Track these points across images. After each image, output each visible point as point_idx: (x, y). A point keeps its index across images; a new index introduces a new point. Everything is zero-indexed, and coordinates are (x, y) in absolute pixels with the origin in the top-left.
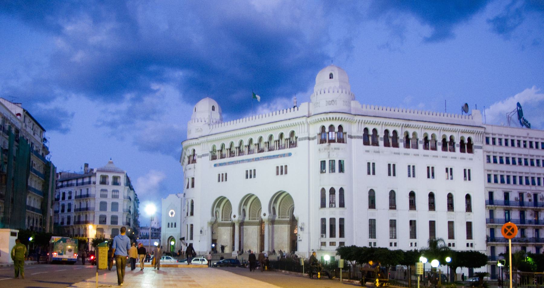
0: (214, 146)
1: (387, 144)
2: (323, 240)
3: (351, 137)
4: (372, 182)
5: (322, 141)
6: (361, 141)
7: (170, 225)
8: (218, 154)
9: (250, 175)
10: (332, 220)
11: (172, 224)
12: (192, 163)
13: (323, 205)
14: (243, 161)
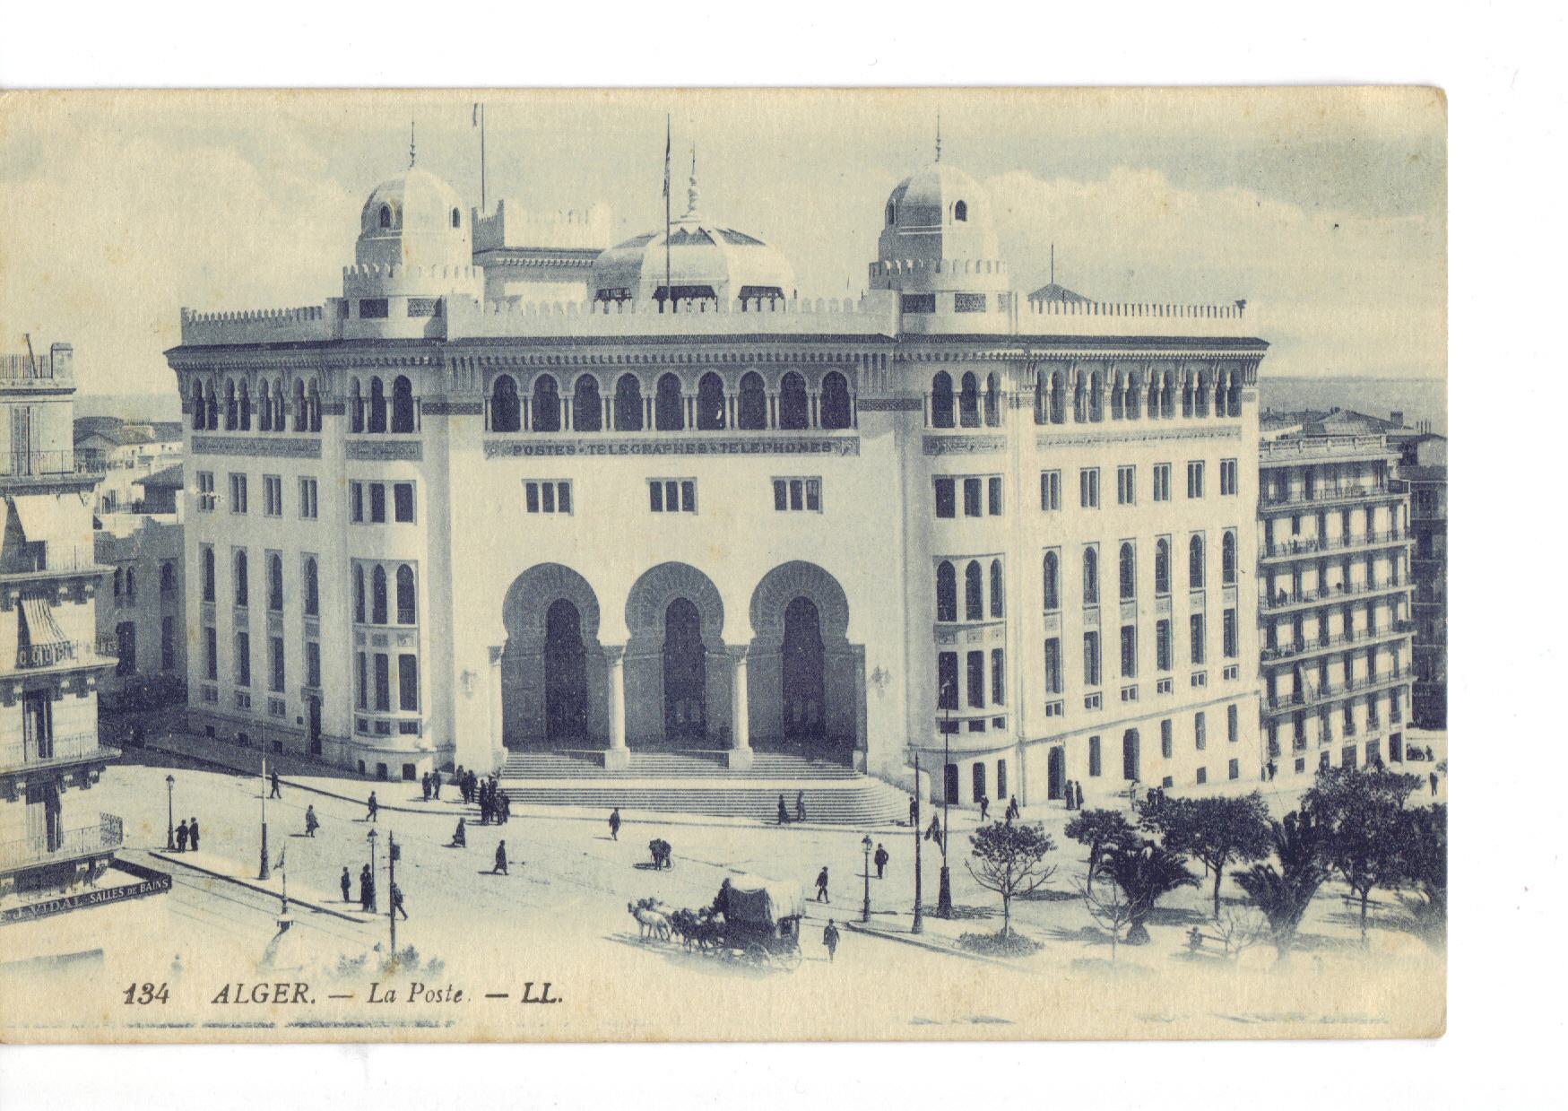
0: (504, 384)
9: (672, 497)
10: (975, 658)
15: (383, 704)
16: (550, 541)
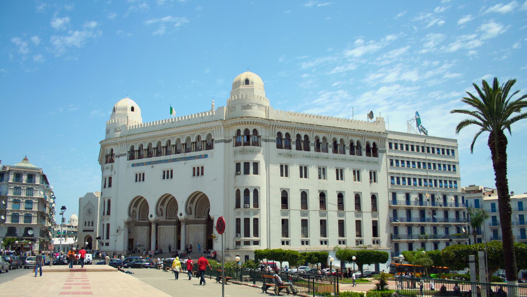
1: (299, 148)
3: (266, 141)
4: (284, 183)
5: (238, 144)
6: (275, 144)
7: (87, 223)
8: (136, 155)
9: (168, 175)
11: (89, 222)
12: (110, 162)
13: (238, 206)
14: (160, 162)
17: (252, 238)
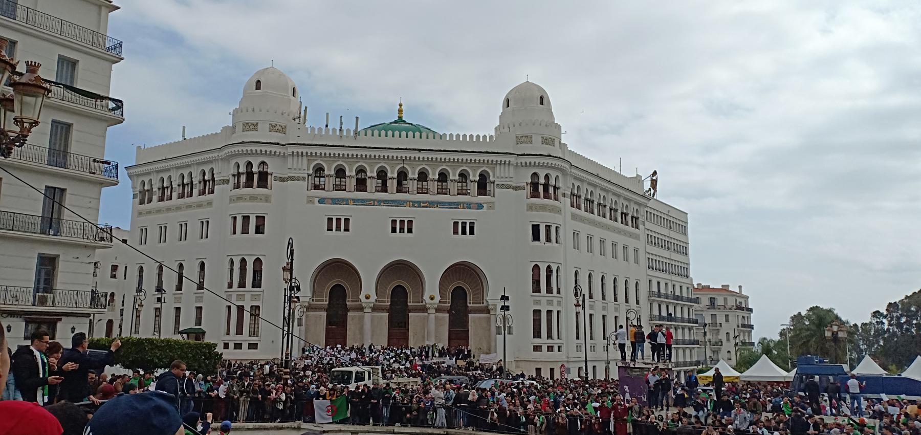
0: (319, 170)
2: (537, 341)
9: (403, 226)
10: (549, 312)
13: (537, 289)
14: (386, 202)
15: (239, 331)
16: (337, 247)
17: (555, 341)
